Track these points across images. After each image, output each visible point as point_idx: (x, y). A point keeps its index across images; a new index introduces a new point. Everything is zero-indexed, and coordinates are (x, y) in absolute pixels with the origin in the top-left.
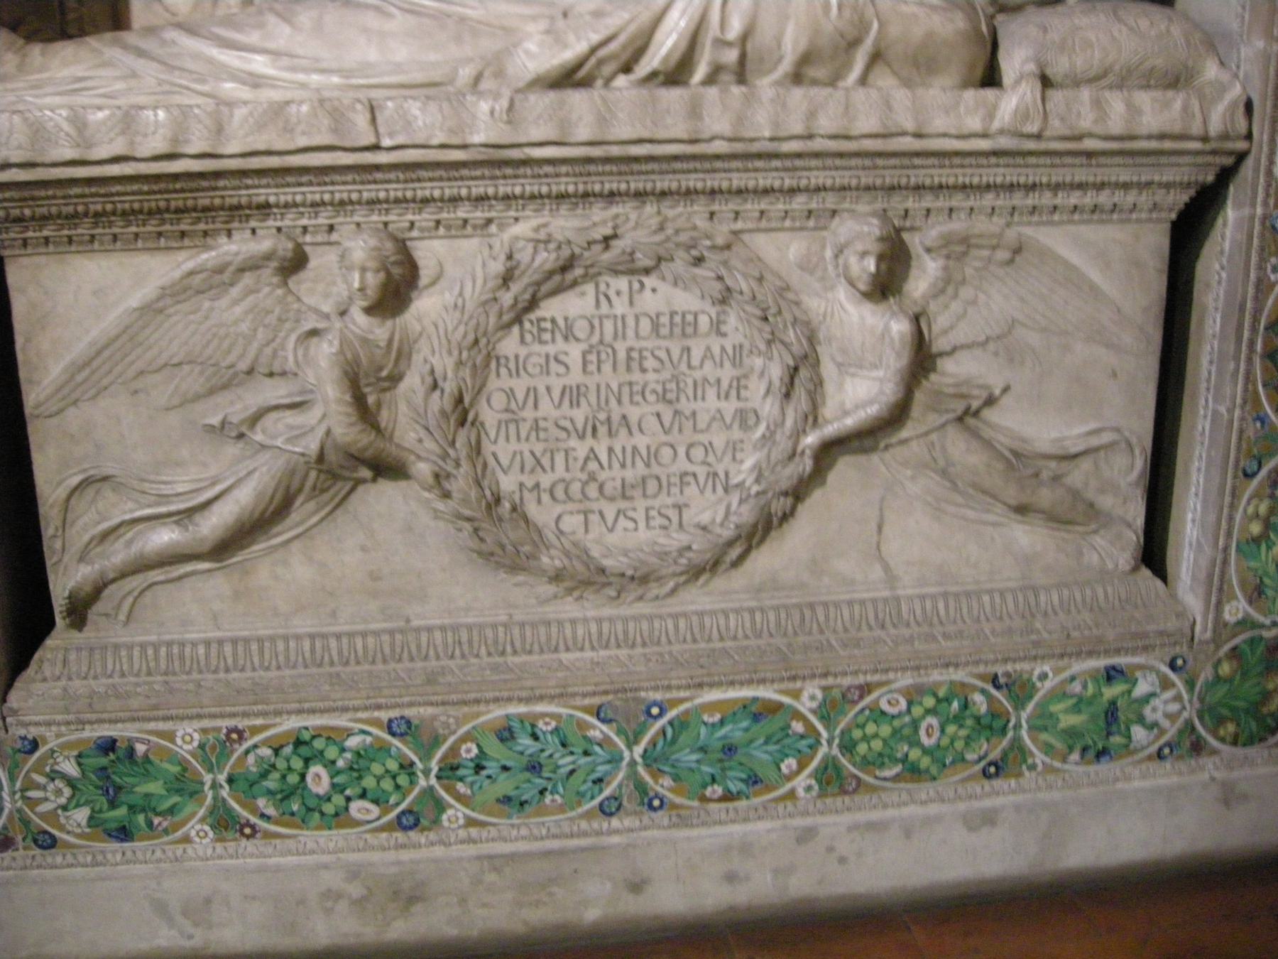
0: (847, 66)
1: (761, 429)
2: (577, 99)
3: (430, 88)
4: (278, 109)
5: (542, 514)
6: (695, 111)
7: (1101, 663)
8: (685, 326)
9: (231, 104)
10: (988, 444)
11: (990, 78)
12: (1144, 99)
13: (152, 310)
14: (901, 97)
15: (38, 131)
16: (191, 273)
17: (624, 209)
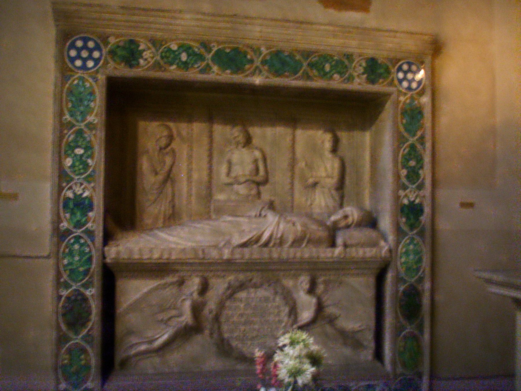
0: (302, 244)
1: (283, 324)
2: (246, 250)
3: (215, 247)
4: (184, 250)
5: (234, 343)
6: (270, 252)
7: (367, 383)
8: (267, 299)
9: (174, 249)
10: (336, 329)
11: (333, 245)
12: (368, 250)
13: (149, 292)
14: (314, 250)
15: (131, 251)
16: (160, 285)
17: (254, 273)
